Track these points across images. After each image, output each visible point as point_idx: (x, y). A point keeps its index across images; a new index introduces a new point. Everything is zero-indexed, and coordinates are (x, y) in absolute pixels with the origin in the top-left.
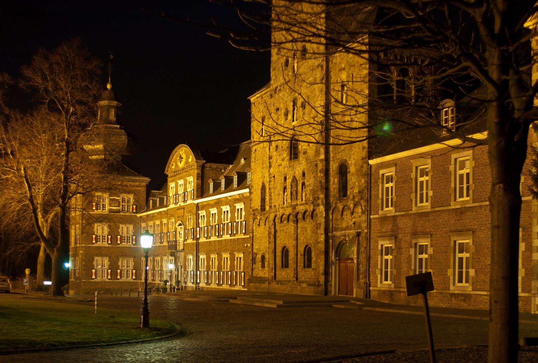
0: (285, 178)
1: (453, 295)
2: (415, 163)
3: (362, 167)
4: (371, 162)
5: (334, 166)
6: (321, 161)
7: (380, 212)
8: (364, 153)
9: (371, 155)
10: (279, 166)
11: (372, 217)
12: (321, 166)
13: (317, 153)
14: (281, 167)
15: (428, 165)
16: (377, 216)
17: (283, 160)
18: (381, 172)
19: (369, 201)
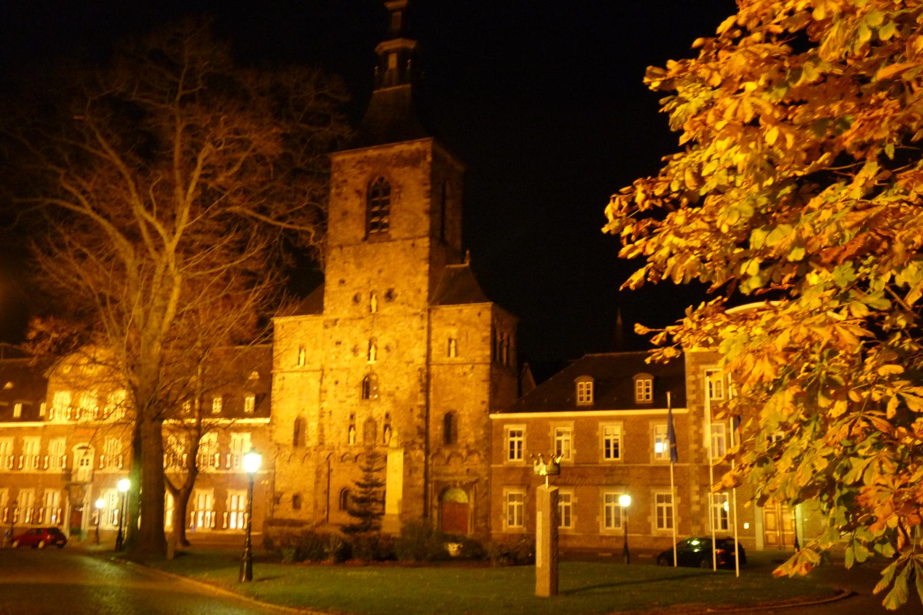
0: (352, 417)
1: (602, 537)
2: (551, 423)
3: (480, 419)
4: (493, 416)
5: (436, 414)
6: (420, 406)
7: (505, 463)
8: (485, 407)
9: (493, 408)
10: (341, 402)
11: (493, 466)
12: (417, 411)
13: (413, 396)
14: (344, 405)
15: (570, 428)
16: (501, 466)
17: (349, 396)
18: (506, 427)
19: (489, 451)
